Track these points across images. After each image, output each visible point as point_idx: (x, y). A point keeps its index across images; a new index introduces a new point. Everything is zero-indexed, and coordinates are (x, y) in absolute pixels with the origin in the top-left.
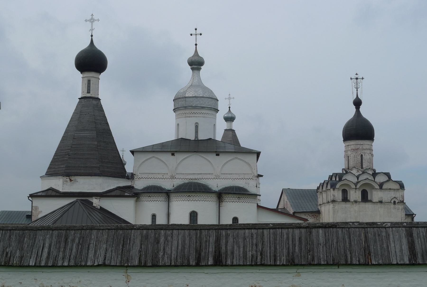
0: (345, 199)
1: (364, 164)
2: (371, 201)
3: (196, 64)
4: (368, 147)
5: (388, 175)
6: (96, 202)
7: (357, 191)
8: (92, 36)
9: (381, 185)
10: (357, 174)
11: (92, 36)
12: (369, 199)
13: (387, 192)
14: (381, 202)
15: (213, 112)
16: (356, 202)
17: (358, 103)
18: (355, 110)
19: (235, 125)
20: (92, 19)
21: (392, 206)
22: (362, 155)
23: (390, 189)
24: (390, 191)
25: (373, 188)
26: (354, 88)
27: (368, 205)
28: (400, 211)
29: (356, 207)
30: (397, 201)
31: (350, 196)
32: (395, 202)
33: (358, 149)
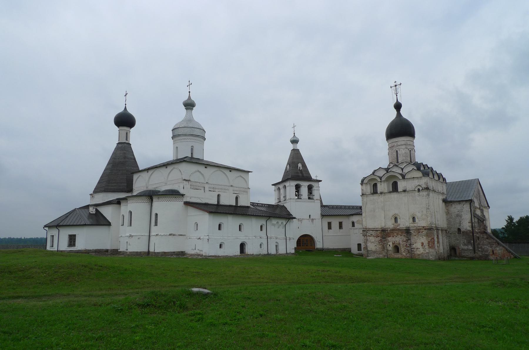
1: (399, 158)
3: (189, 105)
13: (410, 182)
17: (398, 107)
18: (396, 112)
19: (299, 146)
21: (417, 193)
30: (421, 189)
32: (419, 189)
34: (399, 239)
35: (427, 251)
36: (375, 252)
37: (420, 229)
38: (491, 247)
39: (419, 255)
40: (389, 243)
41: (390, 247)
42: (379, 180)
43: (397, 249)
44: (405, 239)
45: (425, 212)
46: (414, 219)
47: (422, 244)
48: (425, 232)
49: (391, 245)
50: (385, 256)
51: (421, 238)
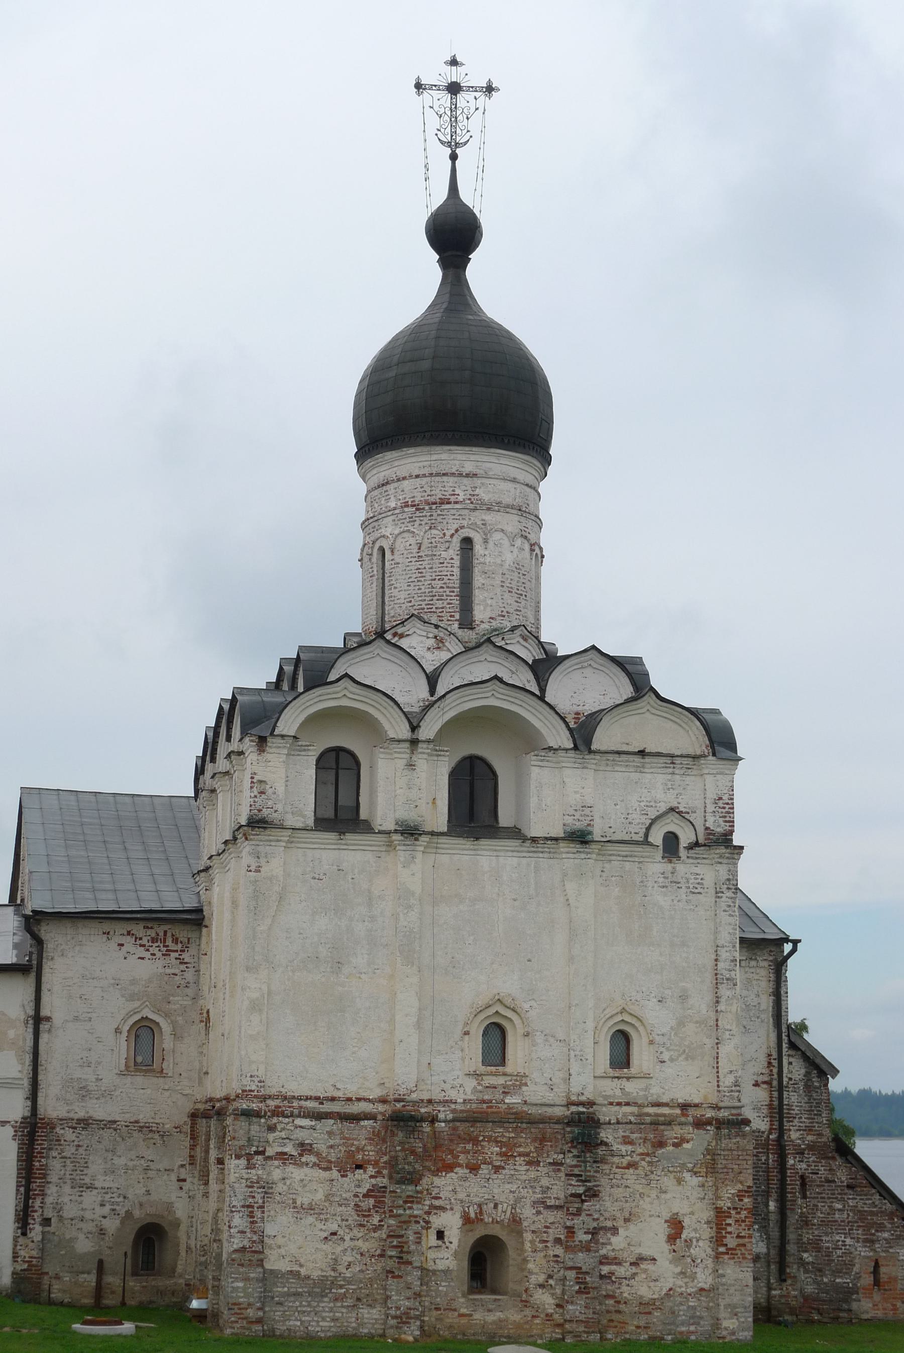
0: (342, 816)
1: (479, 596)
2: (515, 833)
4: (509, 493)
5: (633, 671)
7: (422, 763)
9: (583, 733)
10: (431, 661)
12: (505, 818)
13: (620, 776)
14: (580, 838)
16: (410, 831)
17: (454, 235)
18: (435, 274)
21: (656, 866)
22: (467, 542)
23: (642, 753)
24: (640, 770)
25: (527, 741)
26: (433, 143)
27: (490, 859)
28: (707, 899)
29: (413, 869)
30: (686, 837)
31: (373, 792)
32: (671, 843)
33: (443, 502)
34: (513, 1190)
35: (704, 1279)
36: (322, 1288)
37: (669, 1122)
38: (870, 1242)
39: (647, 1307)
40: (438, 1221)
41: (447, 1257)
42: (403, 731)
43: (484, 1262)
44: (559, 1189)
45: (700, 1003)
46: (622, 1043)
47: (676, 1227)
48: (698, 1142)
49: (454, 1235)
50: (404, 1319)
51: (668, 1182)
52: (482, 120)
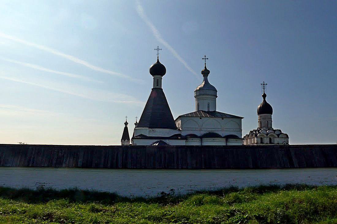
4: (269, 117)
5: (280, 130)
6: (167, 141)
8: (158, 57)
11: (158, 57)
12: (272, 142)
15: (215, 97)
20: (158, 49)
22: (268, 121)
52: (266, 87)
